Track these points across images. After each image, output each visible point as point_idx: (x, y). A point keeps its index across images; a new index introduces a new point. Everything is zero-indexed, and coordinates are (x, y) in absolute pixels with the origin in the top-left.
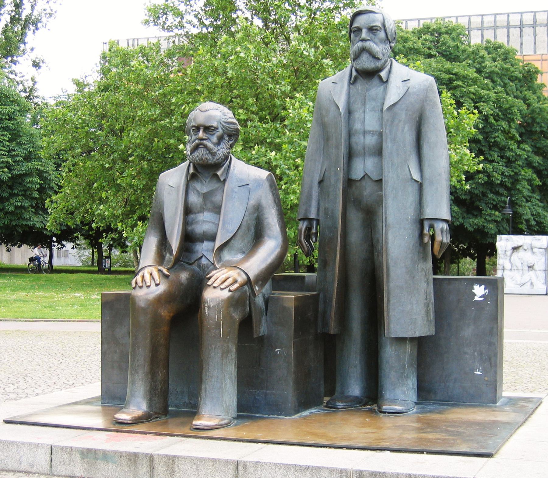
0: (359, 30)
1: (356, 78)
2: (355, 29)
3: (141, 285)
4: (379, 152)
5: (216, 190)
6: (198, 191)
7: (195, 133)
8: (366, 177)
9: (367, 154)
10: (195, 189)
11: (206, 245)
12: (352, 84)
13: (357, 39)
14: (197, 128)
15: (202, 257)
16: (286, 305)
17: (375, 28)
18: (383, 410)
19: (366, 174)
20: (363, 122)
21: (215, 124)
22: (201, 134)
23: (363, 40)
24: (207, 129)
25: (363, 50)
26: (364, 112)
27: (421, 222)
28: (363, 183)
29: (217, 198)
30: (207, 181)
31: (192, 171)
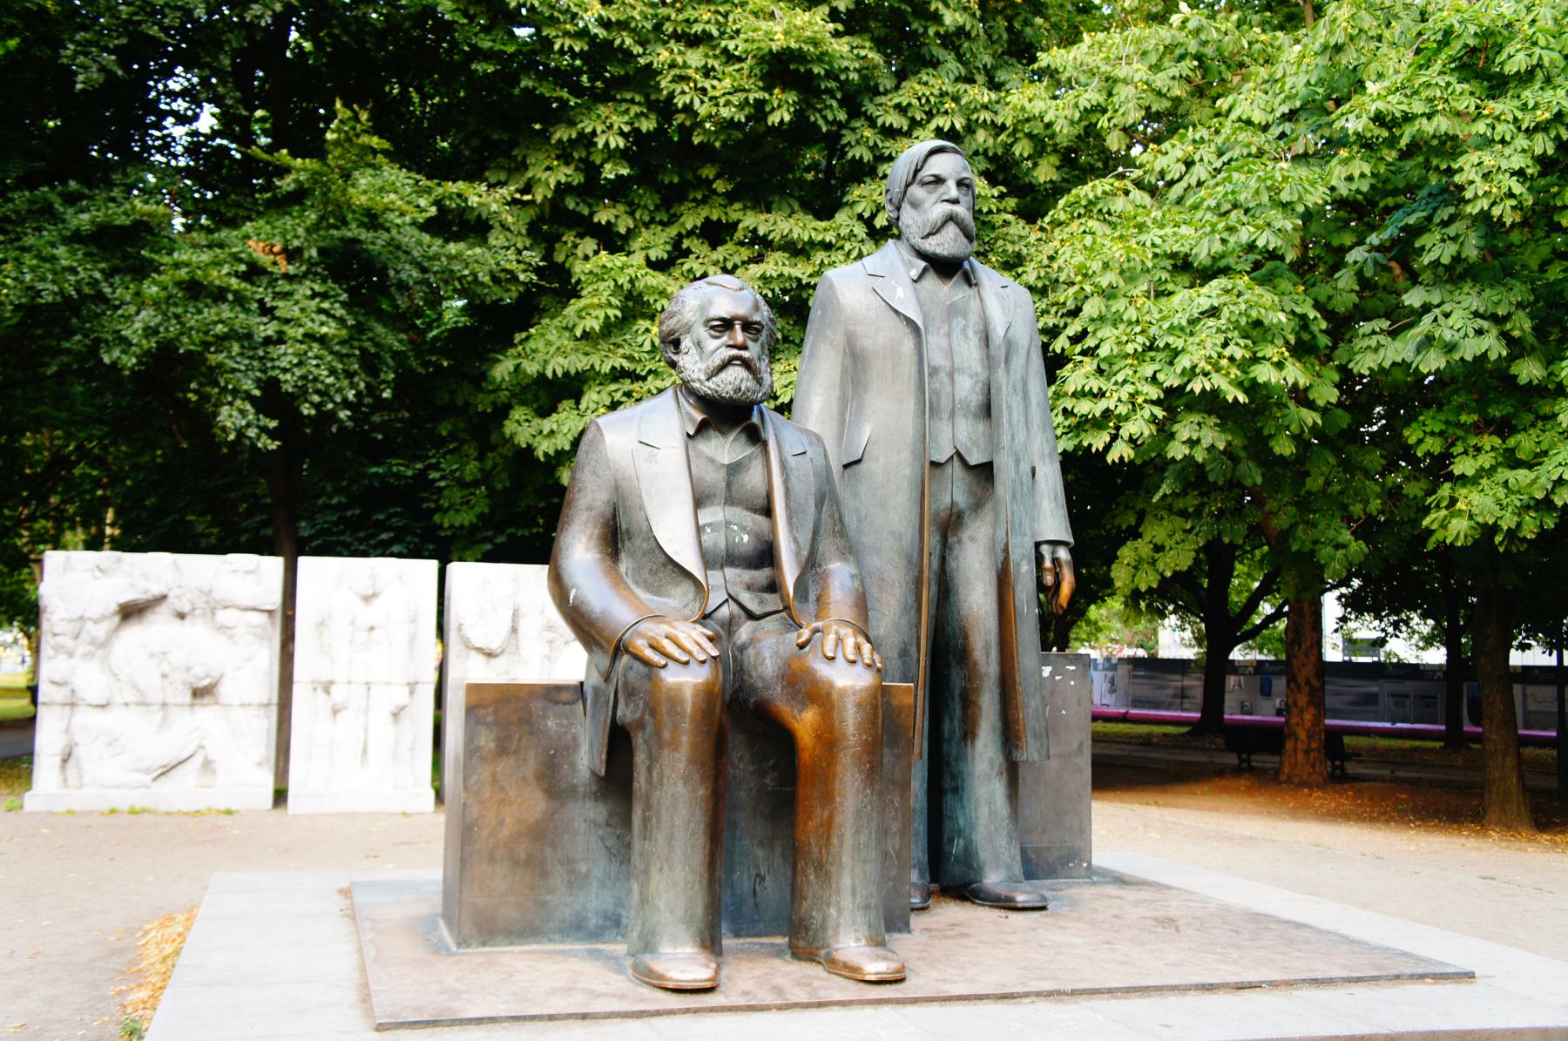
0: (939, 180)
1: (925, 271)
2: (932, 179)
3: (684, 658)
4: (987, 410)
5: (749, 458)
6: (712, 461)
7: (712, 332)
8: (955, 458)
9: (958, 413)
10: (700, 454)
11: (730, 572)
12: (915, 281)
13: (933, 197)
14: (726, 324)
15: (727, 601)
16: (895, 702)
17: (967, 181)
18: (1020, 905)
19: (958, 453)
20: (950, 352)
21: (756, 318)
22: (740, 336)
23: (955, 202)
24: (748, 326)
25: (951, 218)
26: (949, 335)
27: (1038, 545)
28: (949, 470)
29: (753, 479)
30: (732, 436)
31: (699, 417)
